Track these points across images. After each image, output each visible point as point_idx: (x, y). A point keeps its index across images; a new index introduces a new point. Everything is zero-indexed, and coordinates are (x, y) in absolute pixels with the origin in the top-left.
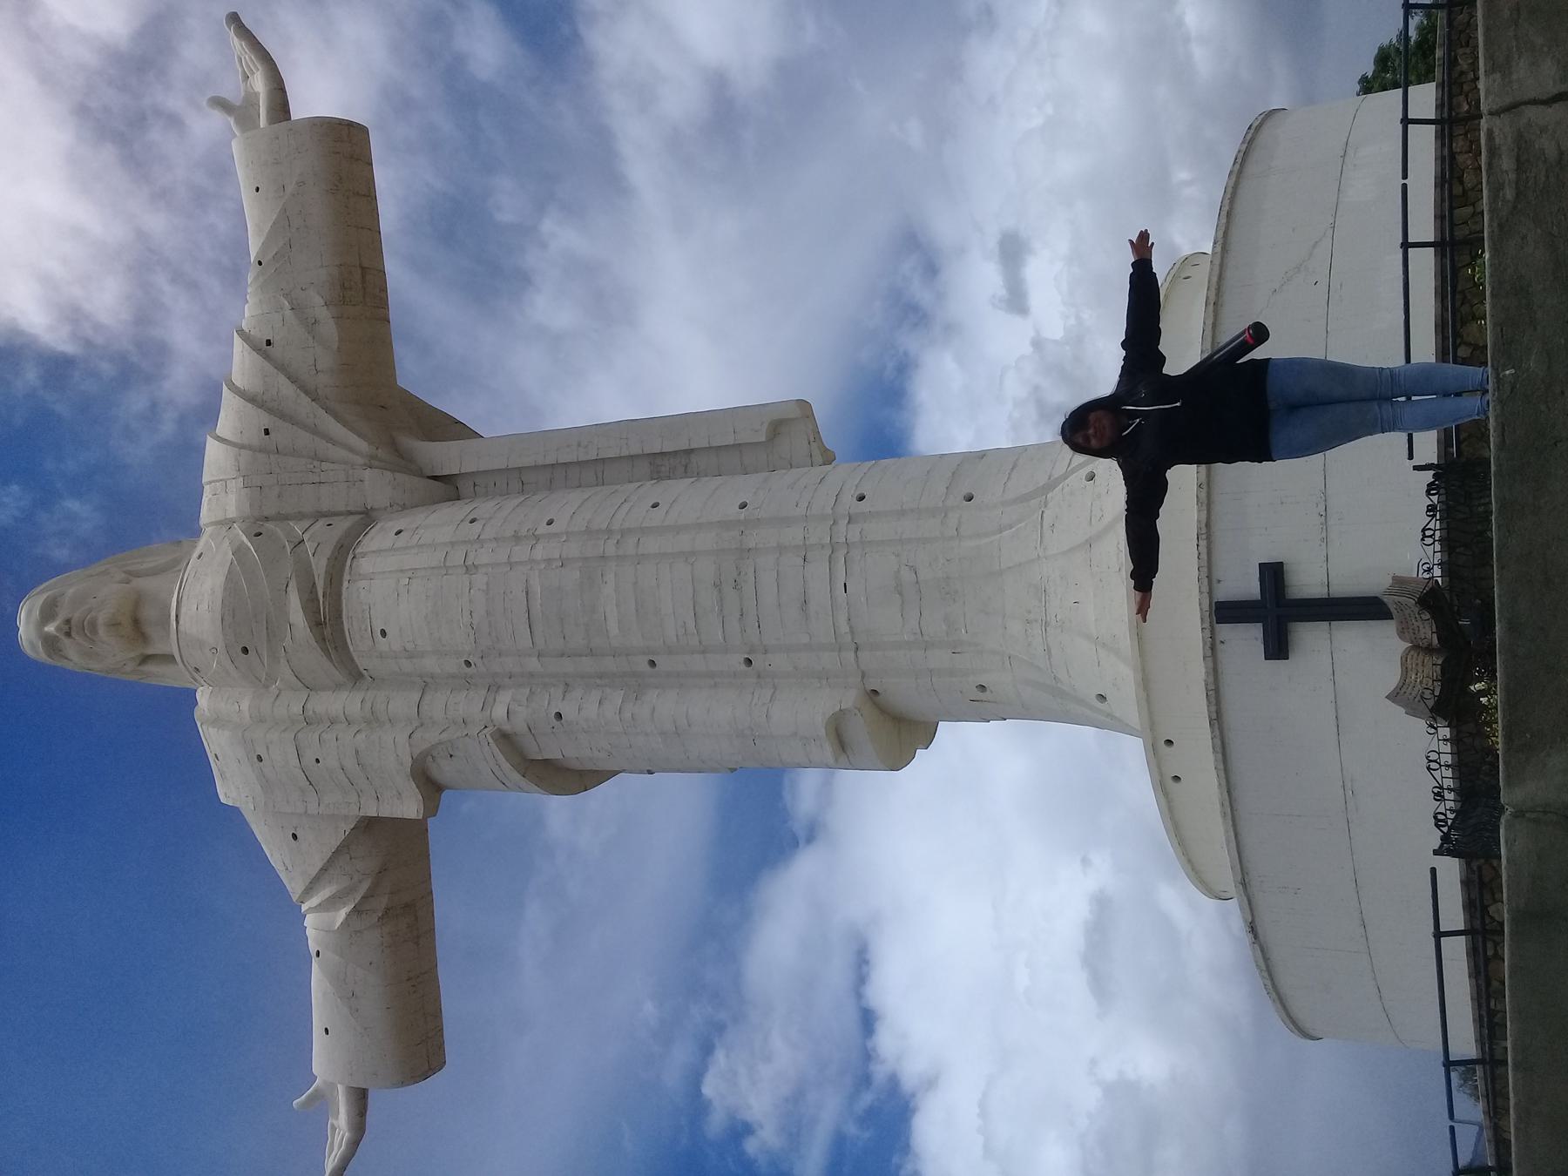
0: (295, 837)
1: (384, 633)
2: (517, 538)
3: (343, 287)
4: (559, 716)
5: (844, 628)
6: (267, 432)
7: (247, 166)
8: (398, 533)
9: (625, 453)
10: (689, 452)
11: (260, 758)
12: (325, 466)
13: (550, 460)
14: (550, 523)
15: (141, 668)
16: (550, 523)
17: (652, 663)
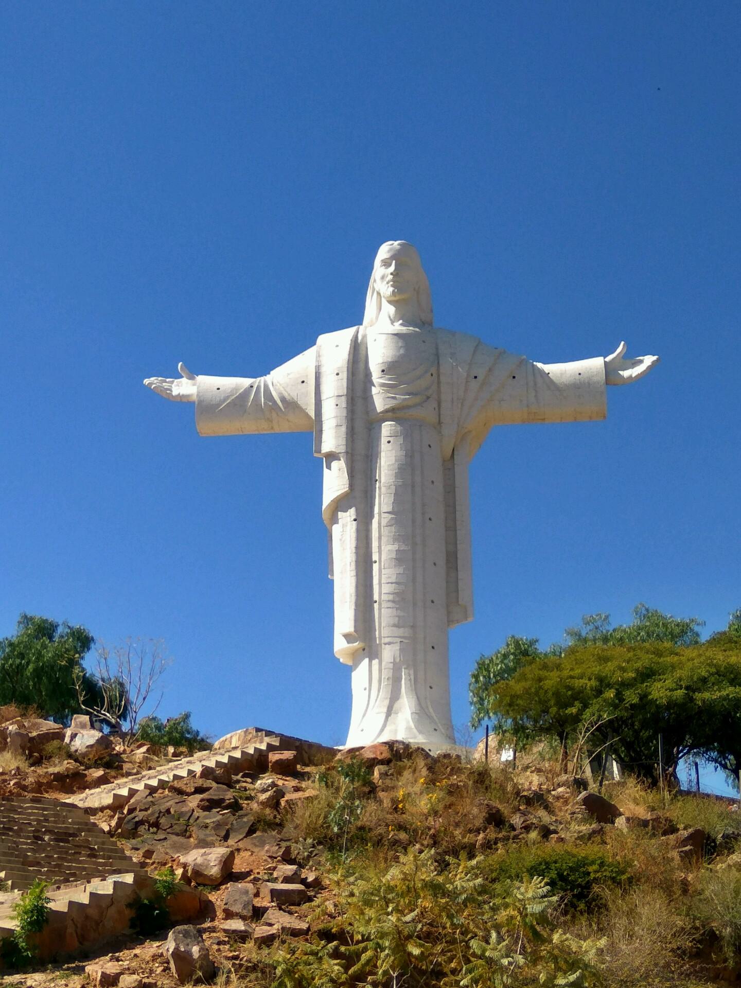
0: (303, 382)
1: (389, 442)
2: (424, 505)
3: (535, 413)
4: (355, 520)
5: (387, 640)
6: (476, 377)
7: (591, 369)
8: (430, 446)
9: (458, 542)
10: (457, 570)
11: (338, 374)
12: (460, 405)
13: (458, 508)
14: (430, 519)
15: (375, 294)
16: (430, 519)
17: (376, 562)
